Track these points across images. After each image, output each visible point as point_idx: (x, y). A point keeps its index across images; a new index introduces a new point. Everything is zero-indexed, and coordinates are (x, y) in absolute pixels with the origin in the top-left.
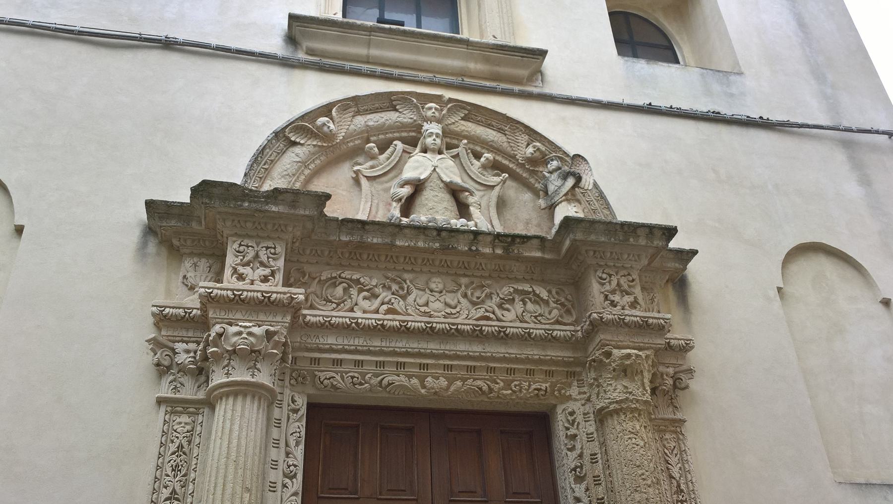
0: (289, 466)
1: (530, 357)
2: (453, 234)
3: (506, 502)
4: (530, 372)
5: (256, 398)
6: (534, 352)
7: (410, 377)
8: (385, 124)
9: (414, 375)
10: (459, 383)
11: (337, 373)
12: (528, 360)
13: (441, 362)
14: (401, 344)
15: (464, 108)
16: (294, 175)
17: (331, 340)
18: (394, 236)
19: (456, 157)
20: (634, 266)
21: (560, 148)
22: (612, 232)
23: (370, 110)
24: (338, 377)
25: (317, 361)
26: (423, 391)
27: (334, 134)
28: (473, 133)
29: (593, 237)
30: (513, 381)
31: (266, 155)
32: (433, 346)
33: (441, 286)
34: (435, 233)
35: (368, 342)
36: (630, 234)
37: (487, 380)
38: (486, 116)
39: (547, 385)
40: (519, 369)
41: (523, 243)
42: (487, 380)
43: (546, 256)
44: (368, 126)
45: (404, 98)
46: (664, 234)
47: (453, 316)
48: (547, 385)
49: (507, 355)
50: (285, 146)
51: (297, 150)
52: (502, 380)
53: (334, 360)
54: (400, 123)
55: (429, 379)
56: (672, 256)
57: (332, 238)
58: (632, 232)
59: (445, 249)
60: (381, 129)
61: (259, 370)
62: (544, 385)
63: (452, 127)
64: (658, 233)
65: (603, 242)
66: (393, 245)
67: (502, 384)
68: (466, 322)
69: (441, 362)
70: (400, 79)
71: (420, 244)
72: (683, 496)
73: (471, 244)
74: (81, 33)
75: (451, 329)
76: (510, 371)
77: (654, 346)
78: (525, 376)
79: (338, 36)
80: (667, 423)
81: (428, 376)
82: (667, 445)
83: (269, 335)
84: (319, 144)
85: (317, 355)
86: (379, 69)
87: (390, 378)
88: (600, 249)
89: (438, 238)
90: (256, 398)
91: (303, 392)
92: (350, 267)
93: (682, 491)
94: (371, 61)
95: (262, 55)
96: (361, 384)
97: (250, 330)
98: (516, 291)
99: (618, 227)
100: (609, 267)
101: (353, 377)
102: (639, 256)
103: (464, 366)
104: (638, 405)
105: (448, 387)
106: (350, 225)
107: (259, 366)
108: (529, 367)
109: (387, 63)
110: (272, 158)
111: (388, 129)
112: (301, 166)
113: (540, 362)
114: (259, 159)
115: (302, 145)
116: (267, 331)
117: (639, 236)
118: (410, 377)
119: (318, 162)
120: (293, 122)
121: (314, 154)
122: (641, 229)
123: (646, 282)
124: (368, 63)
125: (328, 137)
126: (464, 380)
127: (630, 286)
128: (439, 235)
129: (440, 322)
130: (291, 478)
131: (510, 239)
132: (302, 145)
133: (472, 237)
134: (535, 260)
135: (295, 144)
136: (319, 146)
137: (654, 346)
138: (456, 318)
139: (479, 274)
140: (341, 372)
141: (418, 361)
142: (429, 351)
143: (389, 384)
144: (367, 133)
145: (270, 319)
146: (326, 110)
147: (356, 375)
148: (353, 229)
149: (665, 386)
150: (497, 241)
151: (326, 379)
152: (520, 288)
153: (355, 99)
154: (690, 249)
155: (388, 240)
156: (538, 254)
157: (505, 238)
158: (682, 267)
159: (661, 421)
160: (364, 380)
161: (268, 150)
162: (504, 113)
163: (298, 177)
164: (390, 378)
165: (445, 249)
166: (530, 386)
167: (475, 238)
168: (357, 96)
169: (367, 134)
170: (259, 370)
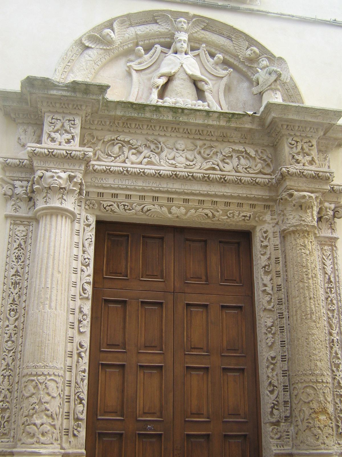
0: (85, 259)
1: (240, 195)
4: (240, 205)
6: (228, 190)
7: (161, 206)
9: (164, 205)
10: (193, 211)
20: (313, 136)
23: (139, 23)
24: (115, 205)
32: (176, 186)
33: (183, 147)
35: (134, 182)
47: (190, 167)
49: (225, 194)
52: (222, 210)
54: (160, 32)
55: (174, 208)
60: (147, 36)
61: (65, 200)
63: (195, 35)
67: (221, 212)
72: (331, 285)
75: (189, 175)
76: (227, 204)
78: (237, 207)
80: (327, 240)
81: (173, 206)
82: (325, 253)
84: (105, 48)
88: (291, 124)
90: (64, 217)
91: (93, 214)
93: (331, 282)
96: (130, 210)
100: (297, 136)
101: (124, 205)
102: (317, 129)
104: (307, 228)
105: (186, 213)
107: (65, 197)
108: (240, 201)
113: (247, 198)
118: (161, 206)
126: (196, 209)
127: (309, 150)
129: (182, 171)
131: (230, 116)
136: (104, 49)
141: (167, 196)
142: (174, 190)
145: (71, 167)
147: (127, 204)
149: (328, 216)
151: (107, 206)
152: (237, 148)
166: (239, 214)
170: (65, 200)
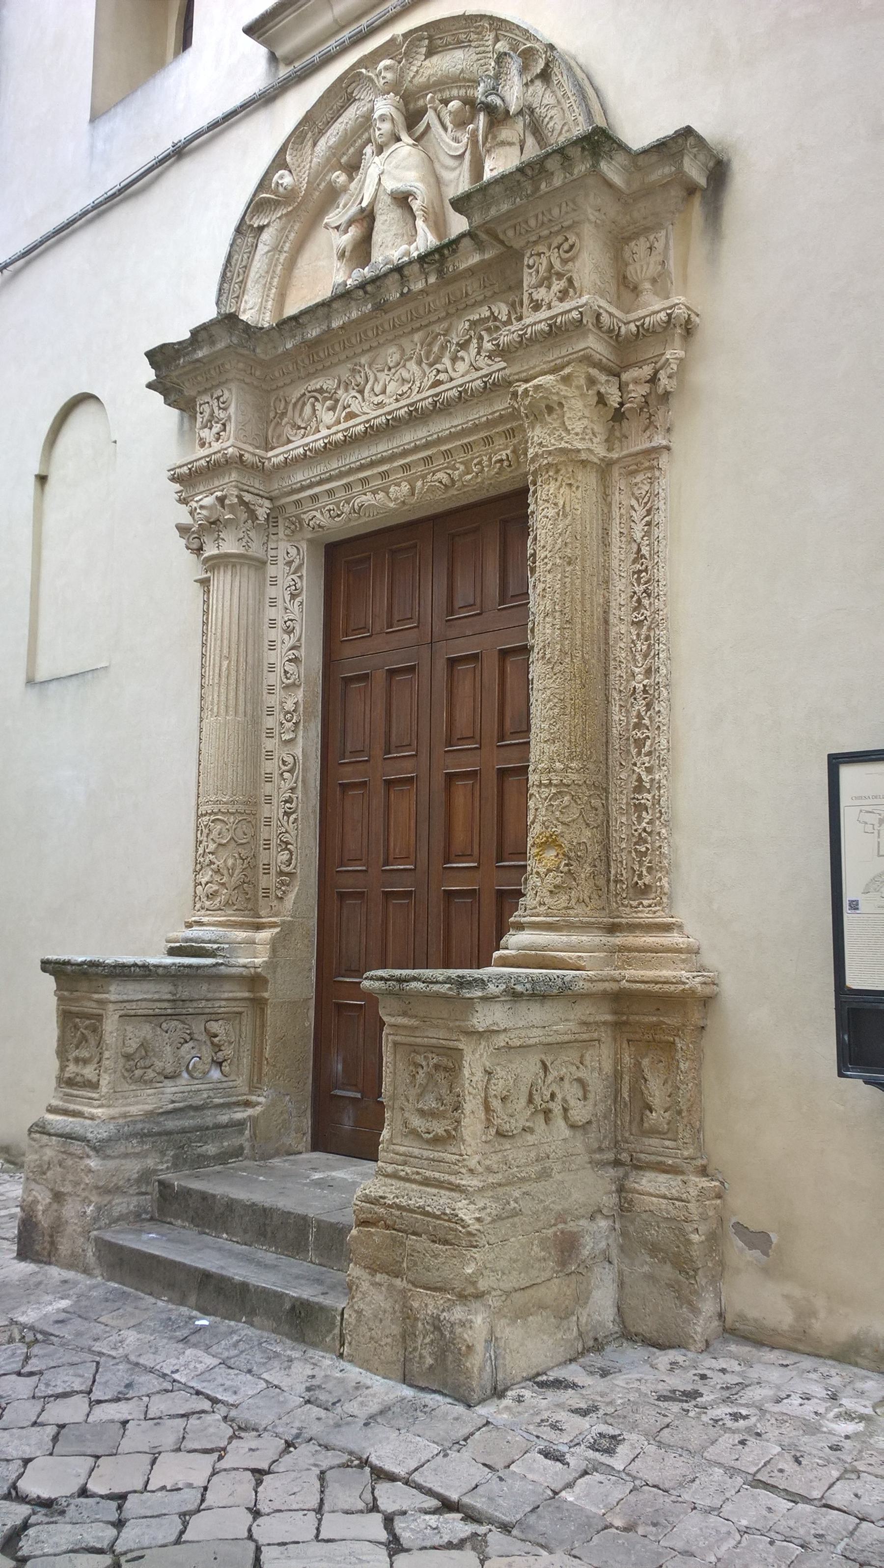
0: (285, 622)
1: (477, 422)
2: (378, 283)
3: (499, 610)
4: (488, 441)
5: (230, 567)
7: (374, 493)
8: (346, 130)
9: (379, 489)
10: (419, 483)
11: (316, 510)
12: (476, 428)
13: (395, 464)
14: (355, 457)
15: (422, 39)
16: (267, 272)
17: (300, 476)
18: (328, 317)
19: (494, 90)
20: (576, 219)
21: (527, 31)
22: (515, 189)
23: (332, 118)
24: (318, 515)
25: (298, 503)
26: (392, 505)
27: (292, 190)
28: (440, 73)
29: (493, 212)
30: (473, 459)
31: (236, 265)
32: (382, 448)
33: (396, 357)
34: (361, 293)
35: (328, 466)
36: (539, 176)
37: (446, 468)
38: (451, 31)
39: (508, 452)
40: (474, 442)
41: (455, 251)
42: (446, 468)
43: (487, 256)
44: (330, 147)
45: (351, 78)
46: (583, 148)
47: (406, 396)
48: (508, 452)
49: (453, 430)
50: (254, 237)
51: (266, 236)
52: (461, 463)
53: (326, 491)
54: (362, 117)
55: (392, 489)
56: (654, 158)
57: (280, 350)
58: (540, 173)
59: (381, 307)
61: (223, 539)
62: (504, 453)
63: (416, 81)
64: (575, 153)
65: (508, 211)
66: (329, 329)
67: (462, 468)
68: (423, 395)
69: (395, 464)
70: (328, 59)
71: (354, 315)
72: (642, 564)
73: (403, 285)
74: (121, 191)
75: (388, 420)
76: (468, 447)
77: (575, 356)
78: (484, 448)
79: (296, 18)
80: (640, 458)
81: (390, 486)
82: (637, 492)
83: (221, 500)
84: (284, 212)
85: (296, 497)
86: (346, 34)
87: (358, 501)
88: (520, 220)
89: (368, 296)
90: (230, 567)
91: (303, 539)
92: (310, 376)
93: (643, 556)
94: (343, 24)
95: (244, 106)
96: (339, 516)
97: (201, 503)
98: (474, 324)
99: (518, 177)
100: (535, 243)
101: (329, 511)
102: (574, 202)
103: (419, 459)
104: (550, 459)
105: (412, 492)
106: (286, 327)
107: (222, 536)
108: (483, 434)
109: (359, 12)
110: (244, 264)
111: (354, 136)
112: (274, 255)
113: (490, 424)
114: (229, 274)
115: (268, 225)
116: (217, 498)
117: (552, 174)
118: (374, 493)
119: (292, 236)
120: (252, 201)
121: (283, 229)
122: (549, 160)
123: (645, 218)
124: (343, 28)
125: (290, 195)
126: (424, 477)
127: (564, 262)
128: (366, 292)
130: (289, 633)
131: (437, 256)
132: (268, 225)
133: (396, 276)
134: (484, 266)
135: (261, 229)
136: (286, 215)
137: (575, 356)
138: (408, 397)
139: (418, 325)
140: (320, 508)
141: (376, 470)
142: (435, 436)
143: (360, 507)
144: (335, 156)
145: (217, 483)
146: (279, 162)
147: (331, 507)
148: (291, 330)
149: (630, 402)
150: (425, 266)
151: (310, 520)
152: (477, 317)
153: (308, 119)
154: (676, 132)
155: (324, 327)
156: (475, 259)
157: (431, 258)
158: (673, 169)
159: (630, 459)
160: (340, 510)
161: (236, 257)
162: (461, 13)
163: (274, 272)
164: (358, 501)
165: (381, 307)
166: (490, 459)
167: (402, 276)
168: (307, 112)
169: (333, 161)
170: (223, 539)
